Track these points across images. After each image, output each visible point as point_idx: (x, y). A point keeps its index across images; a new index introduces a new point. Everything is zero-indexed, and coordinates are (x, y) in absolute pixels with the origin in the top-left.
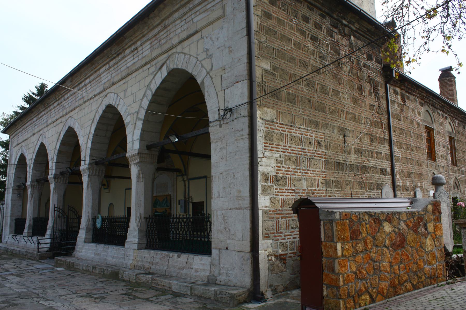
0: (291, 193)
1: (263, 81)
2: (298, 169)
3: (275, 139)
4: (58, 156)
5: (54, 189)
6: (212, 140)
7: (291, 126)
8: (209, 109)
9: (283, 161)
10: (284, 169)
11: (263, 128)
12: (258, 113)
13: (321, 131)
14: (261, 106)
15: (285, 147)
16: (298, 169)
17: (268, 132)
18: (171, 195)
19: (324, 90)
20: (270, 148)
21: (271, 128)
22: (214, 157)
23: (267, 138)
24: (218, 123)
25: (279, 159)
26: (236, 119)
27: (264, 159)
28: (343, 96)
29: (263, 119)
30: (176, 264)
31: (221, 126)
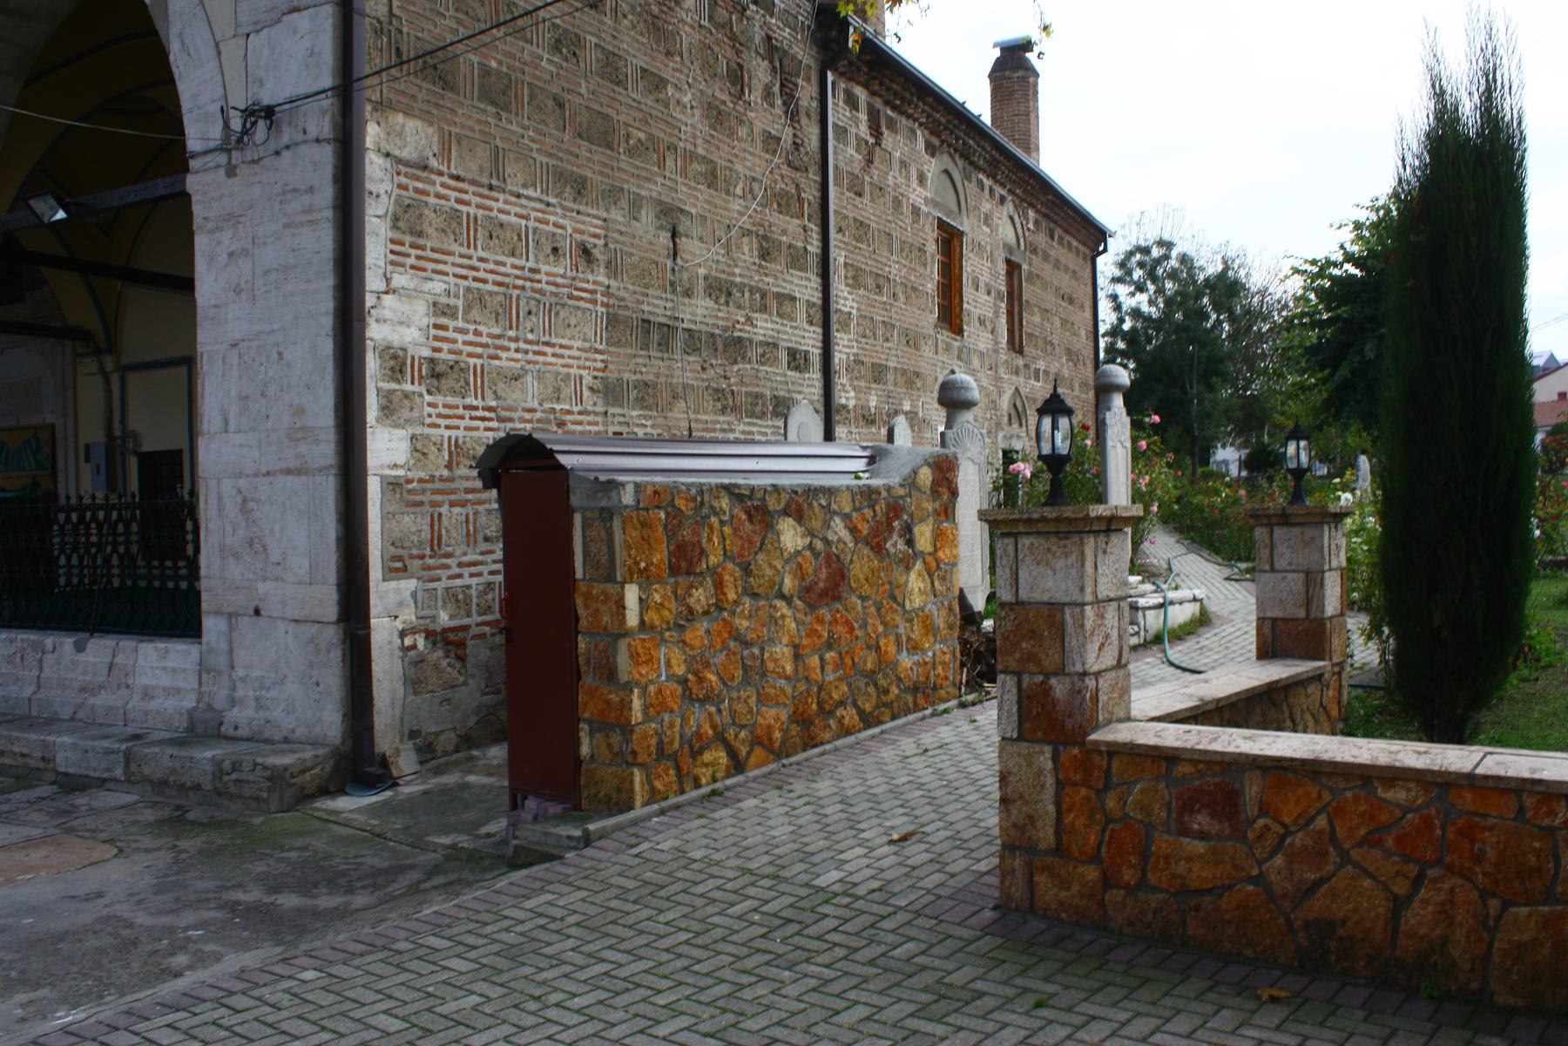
0: (483, 419)
1: (391, 14)
2: (510, 339)
3: (430, 231)
6: (198, 221)
7: (491, 188)
8: (186, 104)
9: (456, 307)
10: (460, 338)
11: (387, 186)
12: (373, 133)
13: (594, 212)
14: (382, 106)
15: (465, 261)
16: (510, 339)
17: (407, 202)
18: (53, 426)
19: (611, 68)
20: (411, 261)
21: (416, 190)
22: (208, 287)
23: (401, 224)
24: (222, 159)
25: (444, 300)
26: (288, 147)
27: (388, 300)
28: (677, 95)
29: (388, 155)
30: (71, 675)
31: (231, 171)
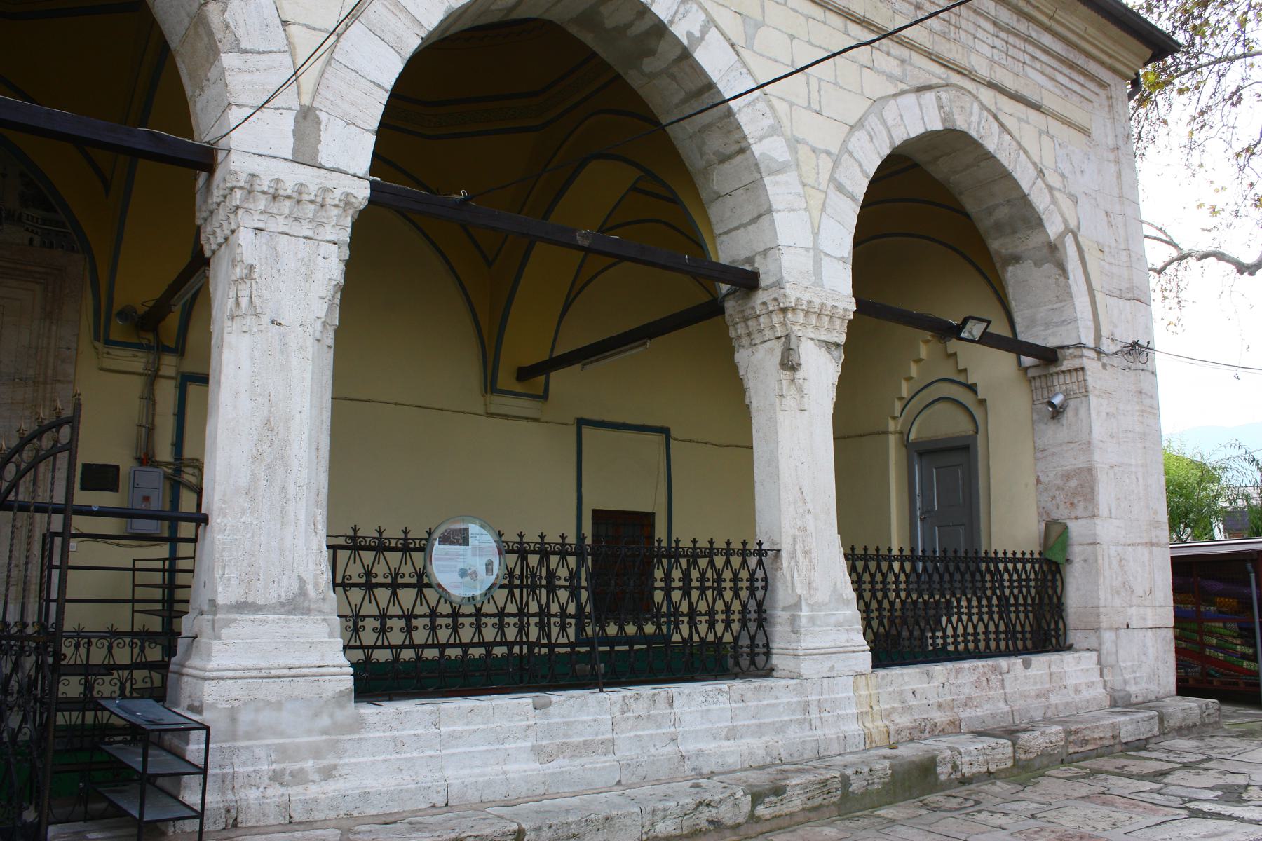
30: (1026, 688)
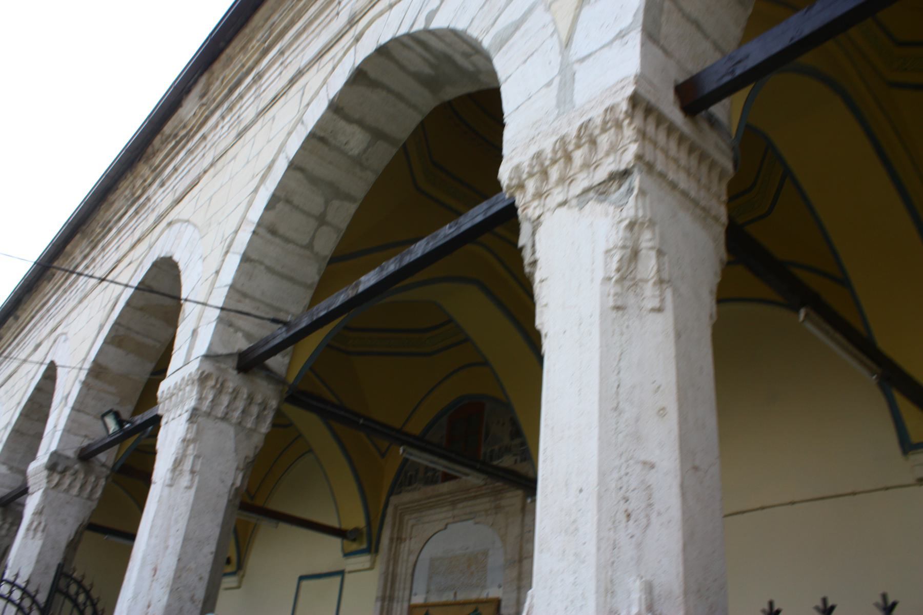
4: (86, 385)
5: (39, 513)
18: (497, 603)
